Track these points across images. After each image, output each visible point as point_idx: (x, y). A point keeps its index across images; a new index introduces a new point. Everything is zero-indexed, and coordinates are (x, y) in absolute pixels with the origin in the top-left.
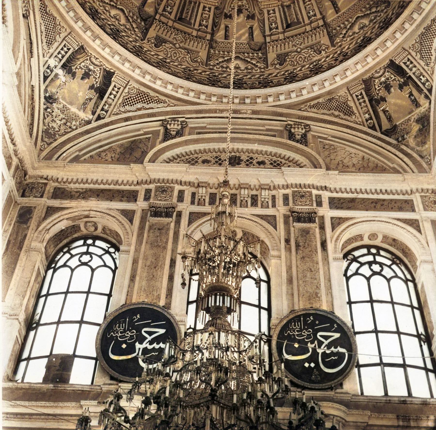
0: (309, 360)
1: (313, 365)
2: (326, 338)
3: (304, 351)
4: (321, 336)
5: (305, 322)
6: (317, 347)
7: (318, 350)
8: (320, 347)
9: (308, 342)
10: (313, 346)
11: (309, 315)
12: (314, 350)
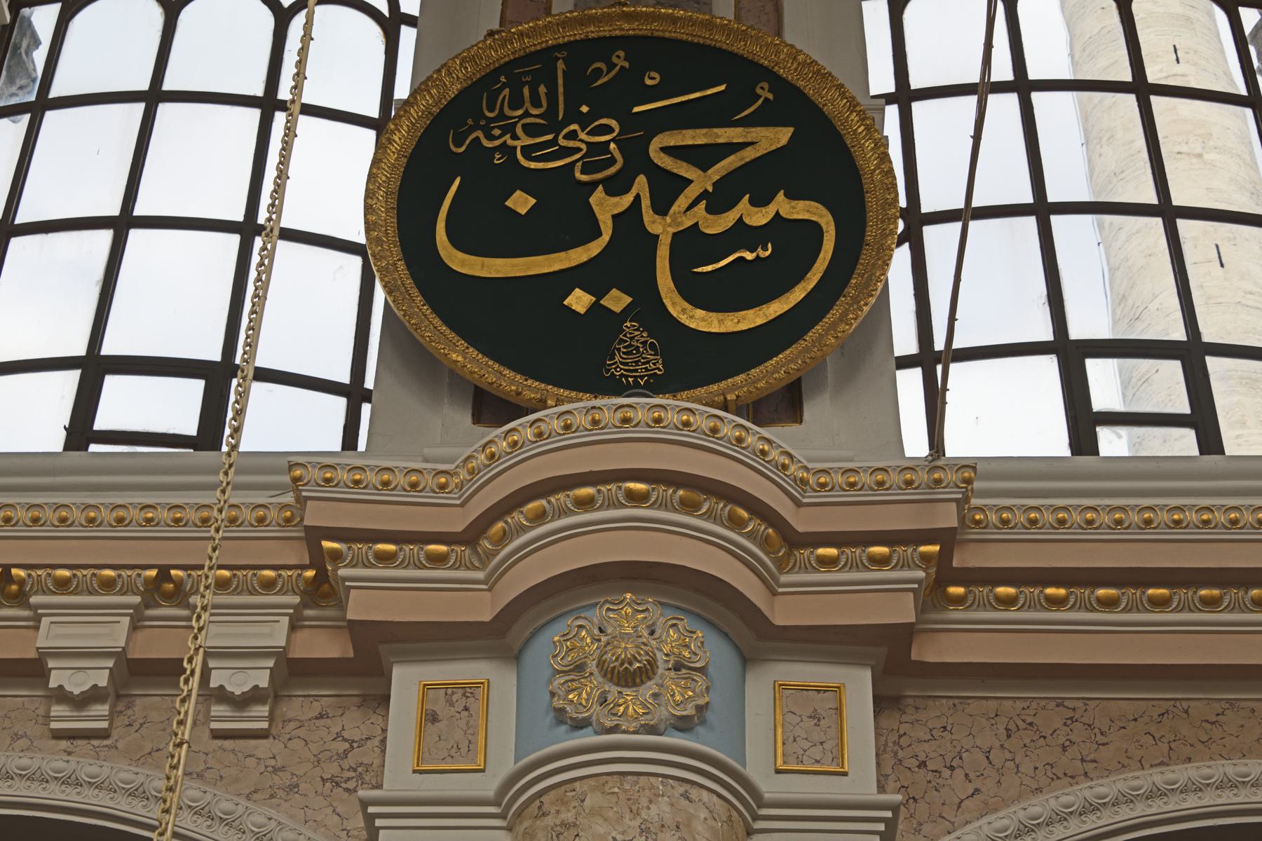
0: (590, 277)
1: (617, 301)
2: (703, 157)
3: (564, 218)
4: (666, 150)
5: (579, 86)
6: (646, 203)
7: (653, 223)
8: (661, 208)
9: (593, 185)
10: (626, 200)
11: (603, 47)
12: (629, 221)
